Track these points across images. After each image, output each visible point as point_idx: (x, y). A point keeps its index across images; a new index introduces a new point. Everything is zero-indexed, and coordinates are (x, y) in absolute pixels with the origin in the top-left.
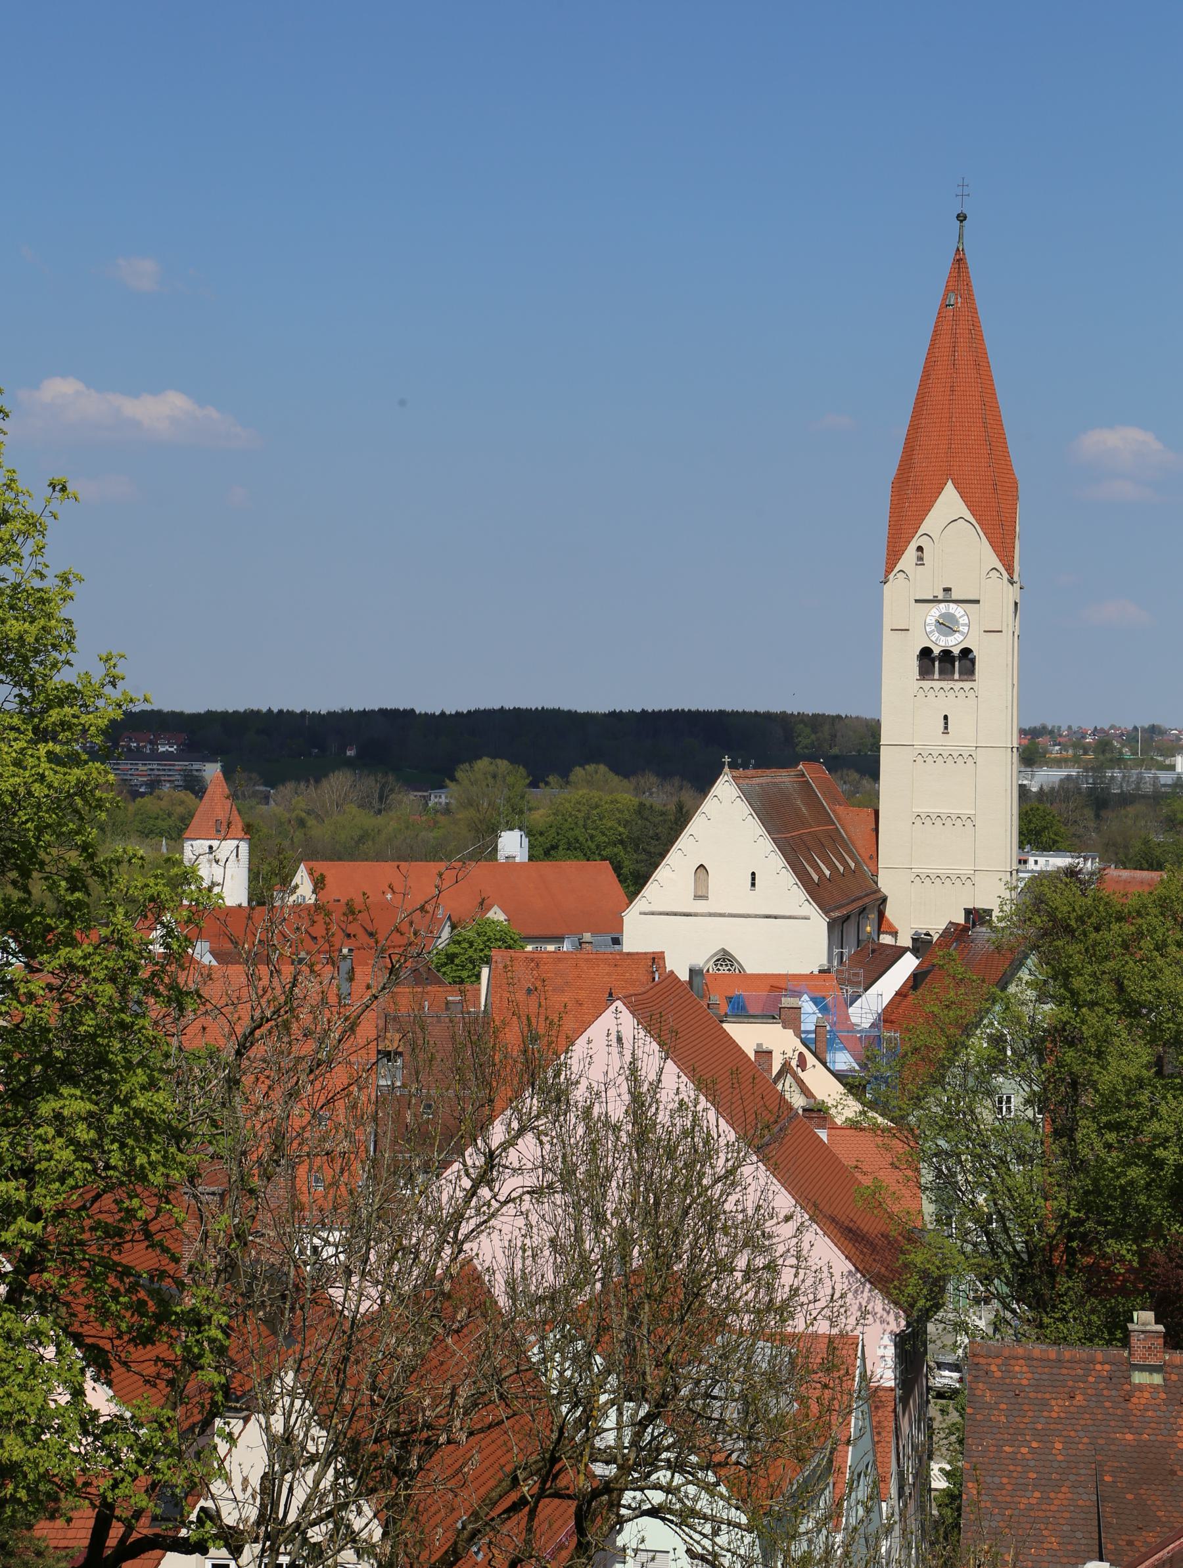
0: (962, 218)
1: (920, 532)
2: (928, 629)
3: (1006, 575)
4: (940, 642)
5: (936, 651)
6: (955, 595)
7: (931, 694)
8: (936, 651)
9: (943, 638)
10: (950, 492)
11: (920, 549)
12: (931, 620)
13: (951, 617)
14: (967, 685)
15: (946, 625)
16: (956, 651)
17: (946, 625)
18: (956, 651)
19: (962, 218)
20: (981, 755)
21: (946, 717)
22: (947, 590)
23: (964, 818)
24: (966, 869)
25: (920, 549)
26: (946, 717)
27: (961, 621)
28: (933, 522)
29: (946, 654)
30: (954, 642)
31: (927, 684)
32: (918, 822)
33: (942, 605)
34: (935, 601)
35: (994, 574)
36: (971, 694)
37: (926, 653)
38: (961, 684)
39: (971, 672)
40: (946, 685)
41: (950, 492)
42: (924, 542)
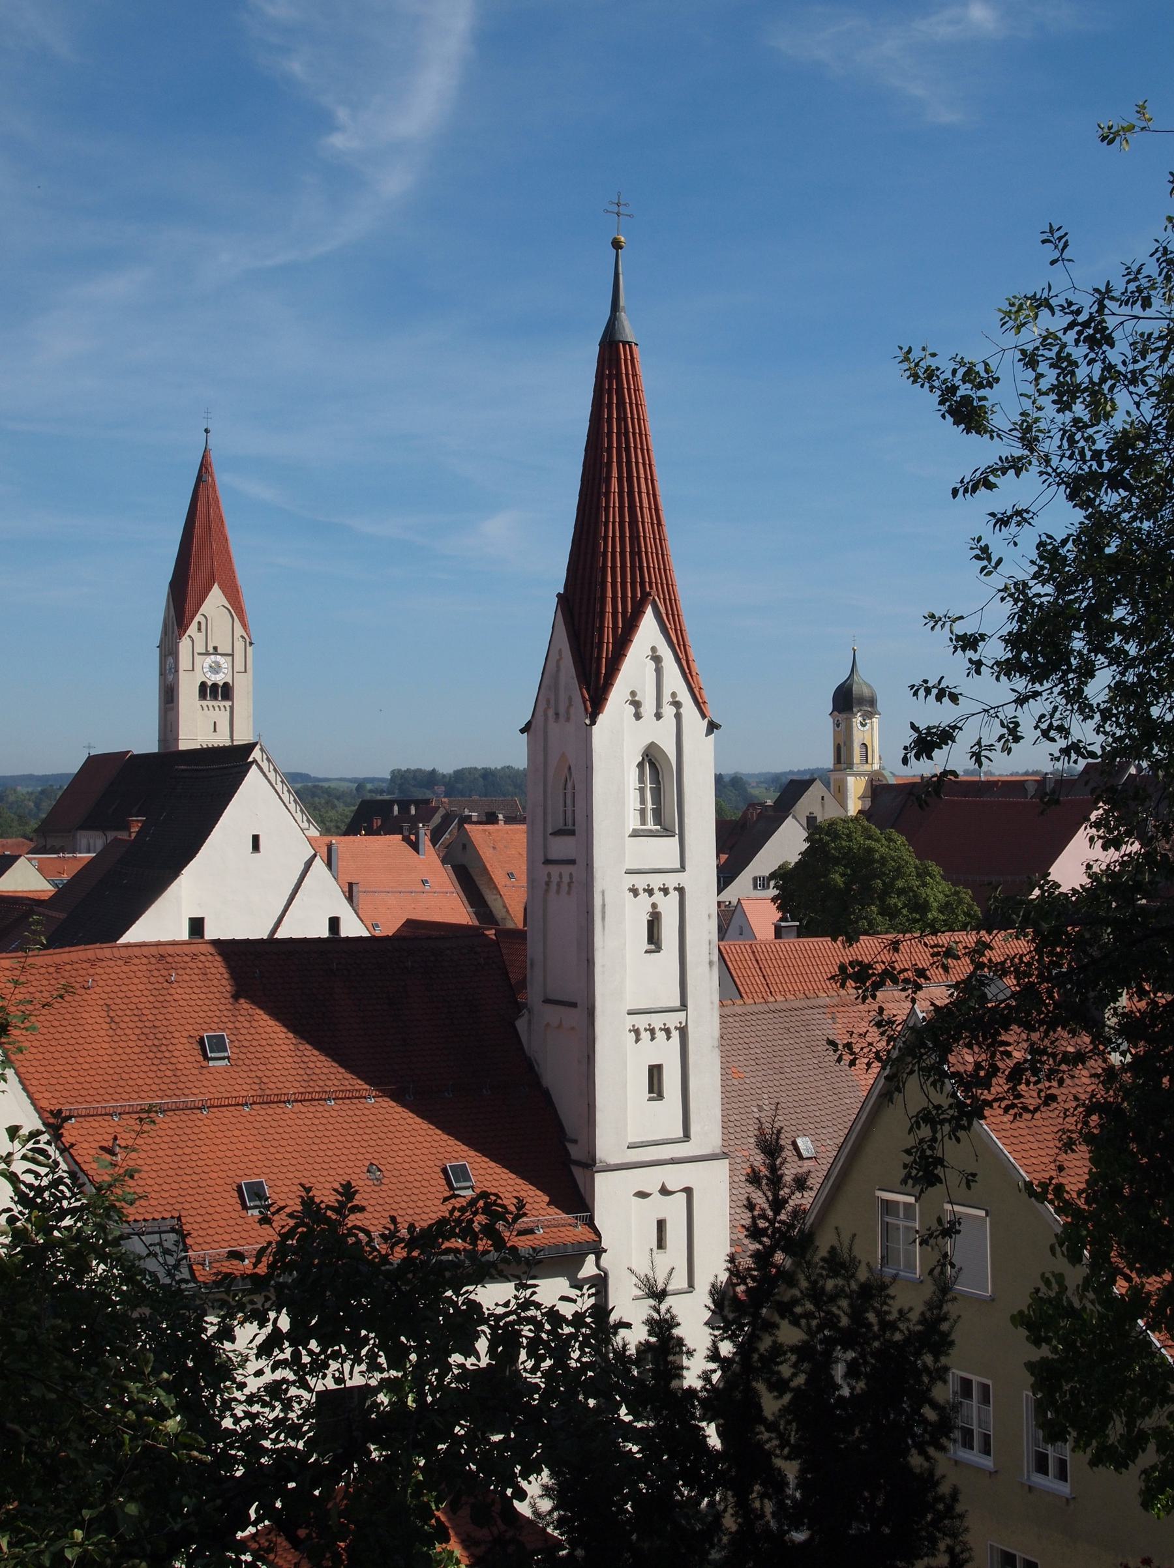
1: (200, 613)
6: (219, 652)
8: (210, 683)
11: (199, 623)
12: (206, 665)
13: (218, 665)
14: (228, 704)
16: (221, 683)
17: (216, 668)
25: (199, 623)
27: (223, 666)
28: (207, 607)
29: (215, 685)
30: (220, 679)
31: (204, 703)
33: (212, 657)
34: (207, 654)
37: (203, 685)
40: (215, 703)
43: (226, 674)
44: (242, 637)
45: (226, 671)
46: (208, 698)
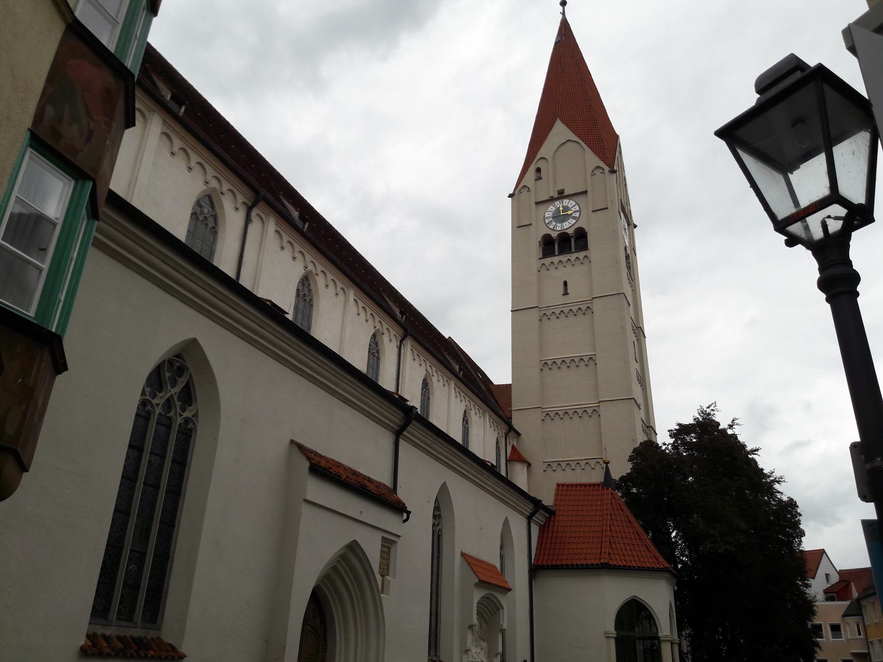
1: (538, 157)
2: (547, 221)
3: (607, 169)
5: (554, 235)
6: (566, 193)
7: (552, 268)
9: (559, 225)
11: (538, 170)
12: (548, 214)
13: (566, 209)
14: (581, 255)
15: (559, 217)
16: (571, 231)
18: (571, 231)
20: (597, 306)
21: (565, 283)
22: (561, 192)
23: (586, 359)
24: (588, 401)
25: (538, 170)
26: (565, 283)
30: (568, 226)
31: (548, 261)
32: (546, 369)
34: (552, 200)
35: (598, 172)
36: (586, 261)
38: (576, 255)
39: (585, 247)
40: (564, 258)
42: (541, 165)
43: (577, 219)
44: (598, 167)
45: (577, 215)
46: (557, 253)
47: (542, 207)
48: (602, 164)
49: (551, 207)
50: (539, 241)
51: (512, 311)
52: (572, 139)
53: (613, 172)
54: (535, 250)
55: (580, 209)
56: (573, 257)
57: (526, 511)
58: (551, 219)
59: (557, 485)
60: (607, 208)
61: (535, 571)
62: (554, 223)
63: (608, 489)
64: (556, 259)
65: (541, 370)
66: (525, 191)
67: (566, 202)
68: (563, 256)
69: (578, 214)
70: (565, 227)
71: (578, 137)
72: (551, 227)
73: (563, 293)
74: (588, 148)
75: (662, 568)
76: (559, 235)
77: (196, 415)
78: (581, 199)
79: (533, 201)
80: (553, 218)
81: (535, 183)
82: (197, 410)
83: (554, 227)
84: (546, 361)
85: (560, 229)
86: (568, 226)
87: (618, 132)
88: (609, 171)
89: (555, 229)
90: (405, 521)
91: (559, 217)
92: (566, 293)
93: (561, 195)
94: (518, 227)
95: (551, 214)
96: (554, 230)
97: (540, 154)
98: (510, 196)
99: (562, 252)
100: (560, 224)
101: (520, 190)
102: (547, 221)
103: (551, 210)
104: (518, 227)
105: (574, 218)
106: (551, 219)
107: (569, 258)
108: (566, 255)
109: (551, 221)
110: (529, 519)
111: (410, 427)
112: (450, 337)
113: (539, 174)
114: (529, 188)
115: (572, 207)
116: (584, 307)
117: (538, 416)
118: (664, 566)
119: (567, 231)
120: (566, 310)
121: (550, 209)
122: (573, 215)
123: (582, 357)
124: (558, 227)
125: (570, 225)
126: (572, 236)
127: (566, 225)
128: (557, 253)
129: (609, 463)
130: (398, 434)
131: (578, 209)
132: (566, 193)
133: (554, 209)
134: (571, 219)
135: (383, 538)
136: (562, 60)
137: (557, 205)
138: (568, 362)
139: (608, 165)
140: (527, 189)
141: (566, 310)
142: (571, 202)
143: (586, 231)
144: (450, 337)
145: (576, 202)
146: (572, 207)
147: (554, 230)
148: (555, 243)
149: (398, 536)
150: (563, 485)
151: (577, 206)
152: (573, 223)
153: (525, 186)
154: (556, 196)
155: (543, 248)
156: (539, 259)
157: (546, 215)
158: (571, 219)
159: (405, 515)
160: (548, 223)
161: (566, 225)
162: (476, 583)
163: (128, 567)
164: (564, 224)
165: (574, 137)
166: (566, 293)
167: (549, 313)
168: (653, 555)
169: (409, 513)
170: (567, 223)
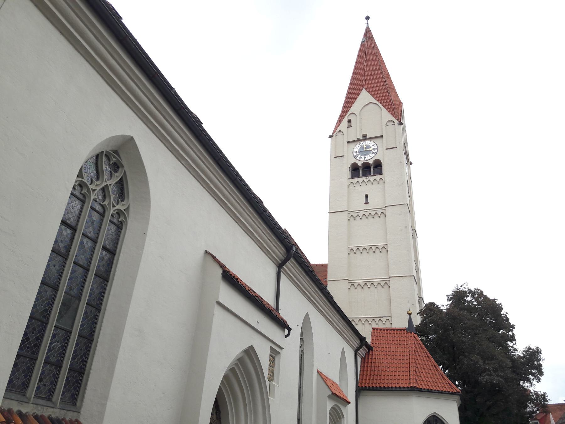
0: (368, 18)
1: (349, 113)
3: (396, 122)
4: (361, 160)
5: (360, 163)
6: (368, 137)
7: (357, 186)
9: (363, 157)
10: (364, 90)
11: (350, 121)
13: (368, 147)
14: (378, 177)
15: (363, 152)
16: (371, 162)
18: (371, 162)
19: (368, 18)
20: (388, 212)
21: (367, 196)
23: (380, 247)
24: (382, 276)
25: (350, 121)
26: (367, 196)
30: (369, 158)
31: (355, 180)
32: (352, 253)
34: (358, 140)
36: (381, 182)
38: (374, 177)
39: (381, 173)
40: (366, 179)
41: (364, 90)
42: (352, 117)
44: (390, 121)
47: (352, 145)
48: (393, 119)
49: (358, 145)
50: (349, 167)
51: (329, 213)
52: (373, 102)
53: (401, 124)
54: (347, 173)
55: (378, 147)
56: (372, 178)
57: (355, 345)
58: (358, 153)
59: (372, 329)
60: (396, 147)
61: (360, 390)
62: (359, 156)
63: (411, 333)
64: (360, 180)
65: (349, 254)
66: (340, 134)
67: (368, 142)
68: (366, 178)
69: (376, 150)
70: (367, 159)
71: (377, 101)
72: (358, 158)
73: (365, 202)
74: (384, 108)
75: (456, 392)
76: (363, 164)
77: (127, 209)
78: (378, 141)
79: (346, 141)
80: (359, 152)
81: (347, 129)
82: (129, 205)
83: (359, 159)
84: (352, 248)
85: (363, 160)
86: (369, 158)
87: (402, 101)
88: (398, 123)
89: (360, 159)
90: (286, 336)
91: (363, 152)
92: (367, 203)
93: (365, 138)
94: (335, 157)
95: (358, 150)
96: (360, 161)
97: (351, 111)
98: (330, 137)
99: (364, 175)
100: (364, 157)
101: (337, 133)
102: (355, 154)
103: (358, 147)
104: (335, 157)
105: (373, 153)
106: (358, 153)
107: (369, 179)
108: (367, 177)
109: (358, 154)
110: (356, 351)
111: (289, 263)
112: (285, 229)
113: (350, 124)
114: (343, 133)
115: (372, 146)
116: (379, 212)
117: (346, 285)
118: (456, 391)
119: (368, 161)
120: (367, 214)
121: (357, 146)
122: (373, 151)
123: (378, 246)
124: (362, 158)
125: (371, 157)
126: (371, 165)
127: (368, 157)
128: (361, 175)
129: (411, 314)
130: (280, 266)
131: (376, 147)
132: (368, 137)
133: (360, 146)
134: (371, 154)
135: (271, 348)
136: (366, 53)
137: (362, 144)
138: (368, 249)
139: (397, 120)
140: (342, 133)
141: (367, 214)
142: (372, 142)
143: (382, 162)
144: (285, 229)
145: (375, 143)
146: (372, 146)
147: (360, 161)
148: (360, 169)
149: (282, 348)
150: (377, 329)
151: (376, 145)
152: (372, 156)
153: (340, 131)
154: (361, 138)
155: (351, 172)
156: (349, 179)
157: (354, 151)
158: (371, 154)
159: (287, 331)
160: (356, 156)
161: (368, 157)
162: (329, 395)
163: (51, 343)
164: (366, 157)
165: (374, 101)
166: (367, 203)
167: (355, 215)
168: (447, 383)
169: (289, 329)
170: (368, 156)
